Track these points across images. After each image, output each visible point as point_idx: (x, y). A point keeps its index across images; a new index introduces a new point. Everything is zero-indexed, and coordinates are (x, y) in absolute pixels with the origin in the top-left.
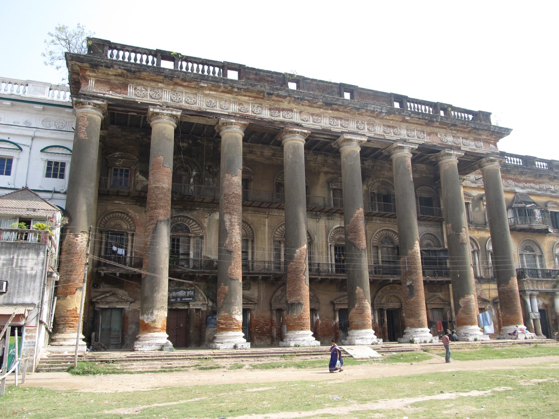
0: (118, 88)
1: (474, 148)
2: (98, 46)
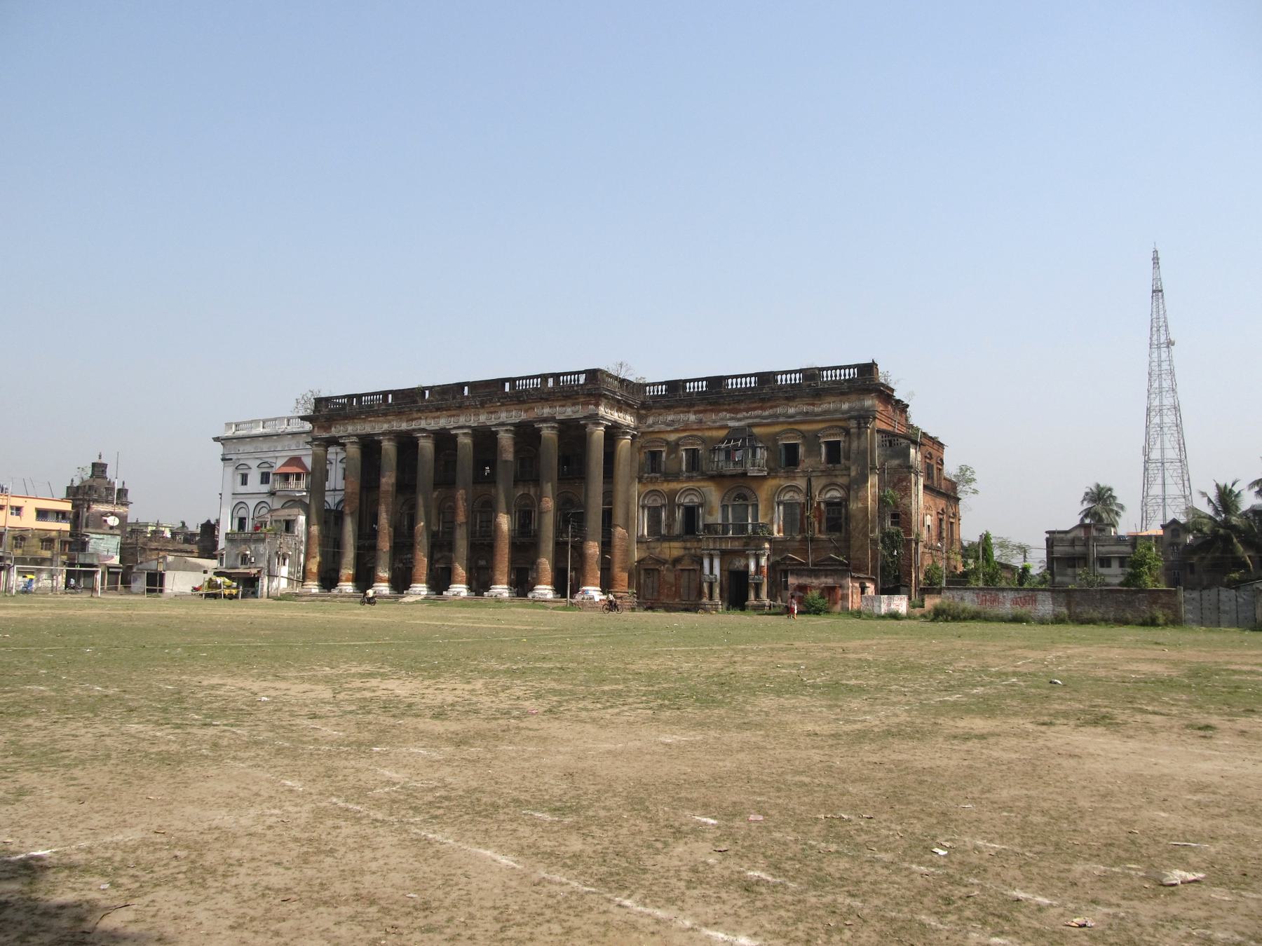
2: (319, 401)
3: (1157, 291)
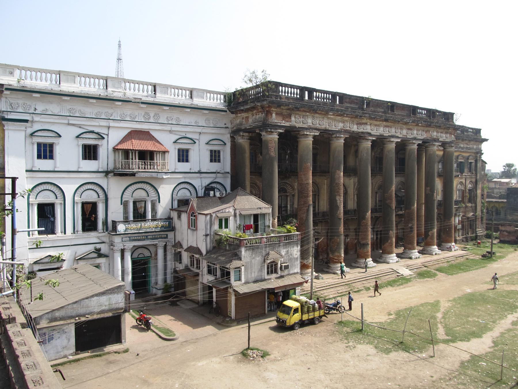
0: (287, 117)
1: (445, 138)
3: (119, 59)
